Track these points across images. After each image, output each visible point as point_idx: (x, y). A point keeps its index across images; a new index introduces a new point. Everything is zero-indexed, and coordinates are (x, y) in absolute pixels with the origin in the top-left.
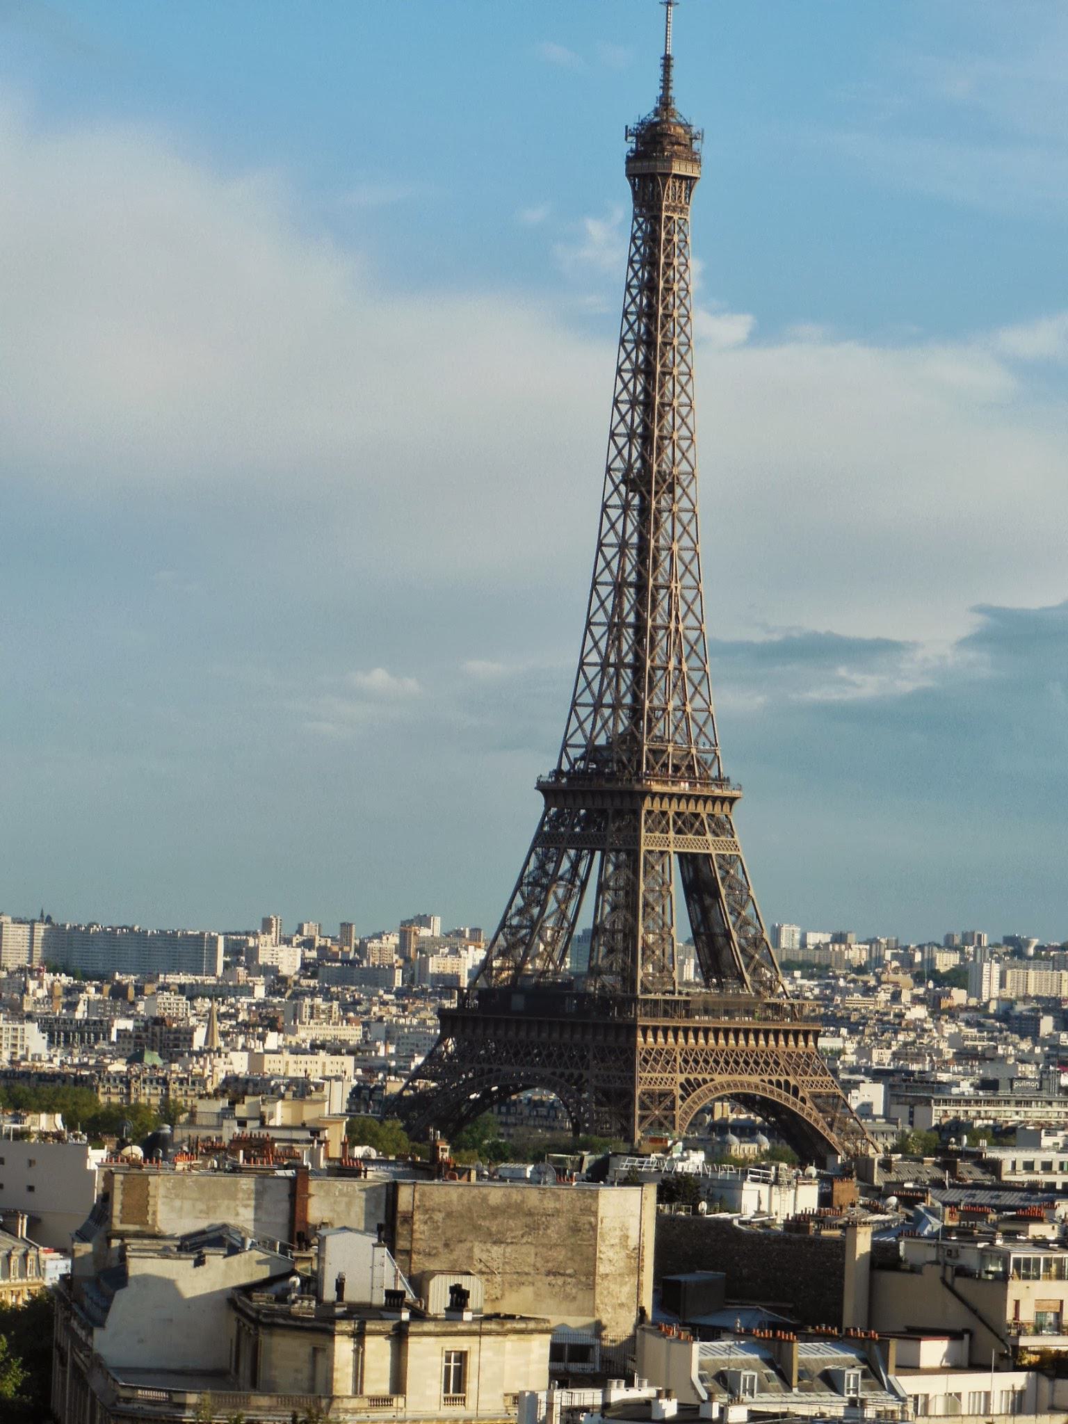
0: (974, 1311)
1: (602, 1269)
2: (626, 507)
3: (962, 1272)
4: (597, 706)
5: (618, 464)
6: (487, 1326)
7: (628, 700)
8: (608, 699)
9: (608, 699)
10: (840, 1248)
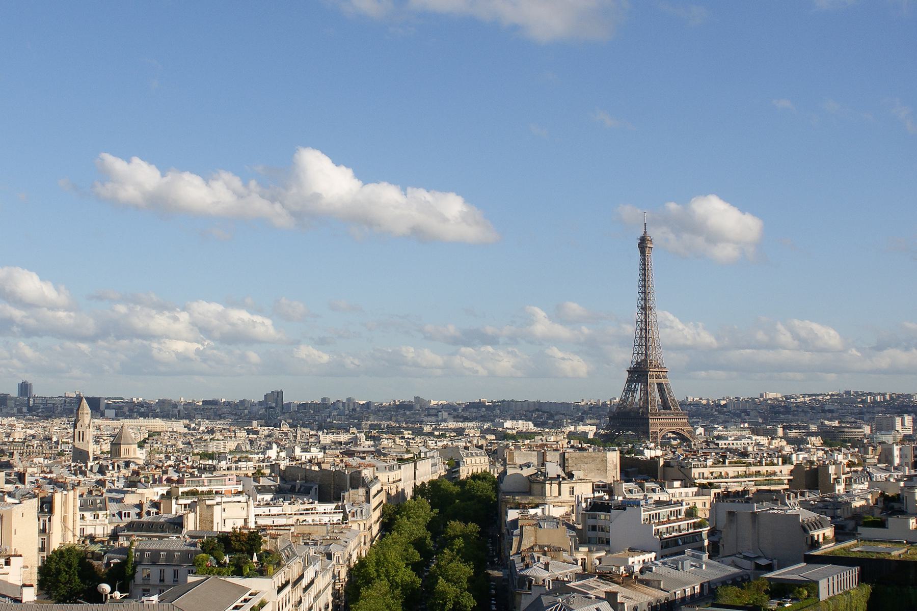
0: (685, 475)
1: (608, 469)
2: (642, 314)
3: (682, 467)
4: (638, 354)
5: (640, 305)
6: (578, 481)
7: (644, 352)
8: (640, 352)
9: (640, 352)
10: (657, 463)
